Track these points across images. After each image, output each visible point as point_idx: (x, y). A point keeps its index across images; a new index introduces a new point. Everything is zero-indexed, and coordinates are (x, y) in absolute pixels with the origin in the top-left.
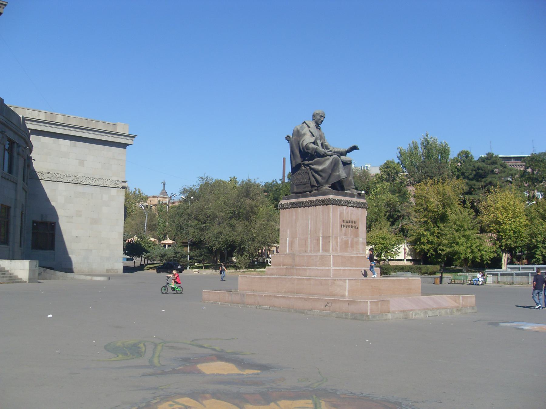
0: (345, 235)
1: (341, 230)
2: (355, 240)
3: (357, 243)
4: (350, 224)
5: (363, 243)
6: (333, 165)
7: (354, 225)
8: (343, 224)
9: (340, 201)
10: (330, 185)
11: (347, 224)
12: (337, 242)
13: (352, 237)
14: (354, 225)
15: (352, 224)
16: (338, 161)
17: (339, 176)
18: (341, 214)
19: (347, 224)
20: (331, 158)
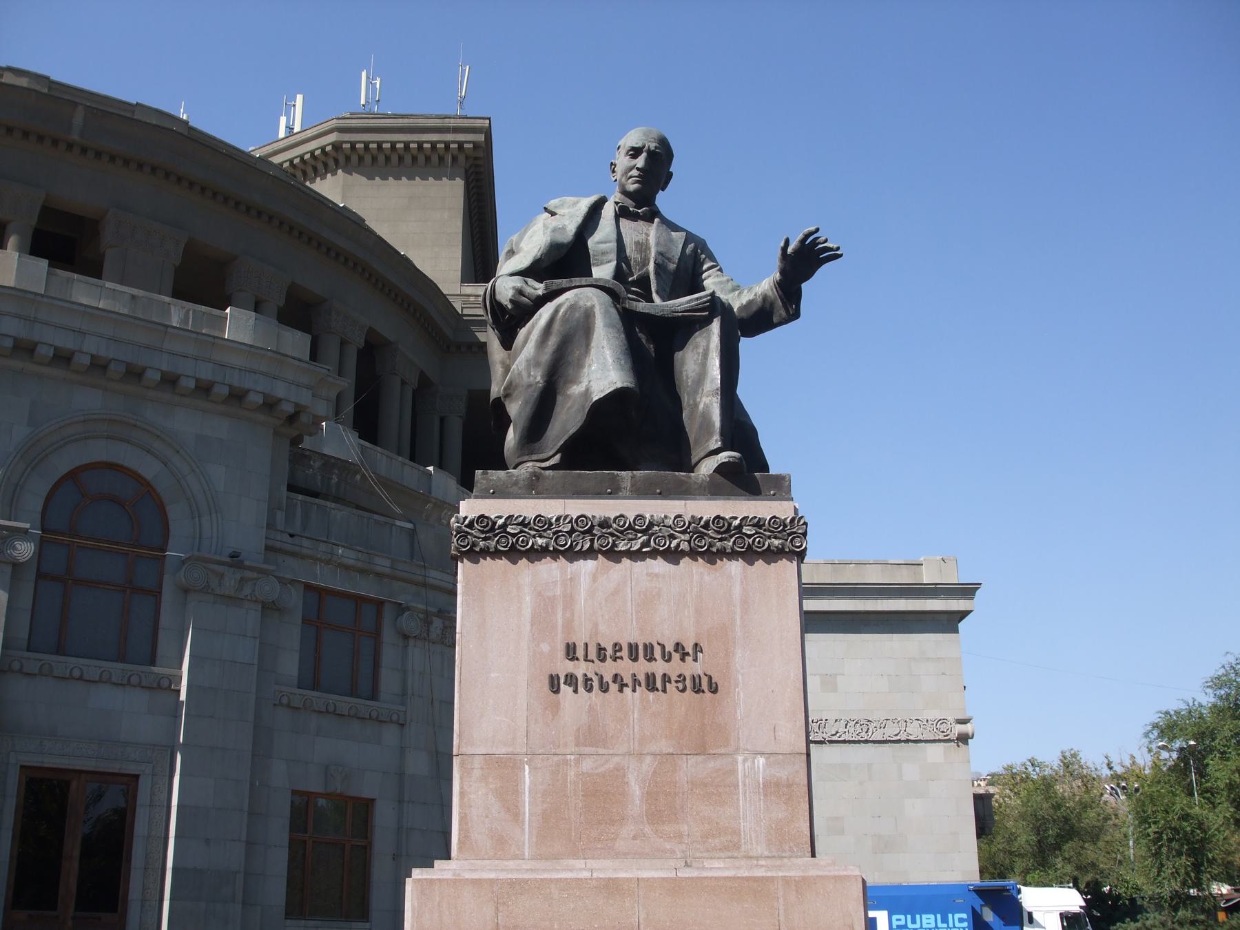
0: (592, 736)
1: (556, 708)
2: (691, 768)
3: (720, 789)
4: (626, 668)
5: (772, 788)
6: (553, 341)
7: (675, 667)
8: (564, 667)
9: (543, 524)
10: (557, 459)
11: (608, 669)
12: (509, 797)
13: (664, 746)
14: (675, 667)
15: (659, 667)
16: (588, 315)
17: (587, 392)
18: (544, 605)
19: (608, 669)
20: (545, 313)
